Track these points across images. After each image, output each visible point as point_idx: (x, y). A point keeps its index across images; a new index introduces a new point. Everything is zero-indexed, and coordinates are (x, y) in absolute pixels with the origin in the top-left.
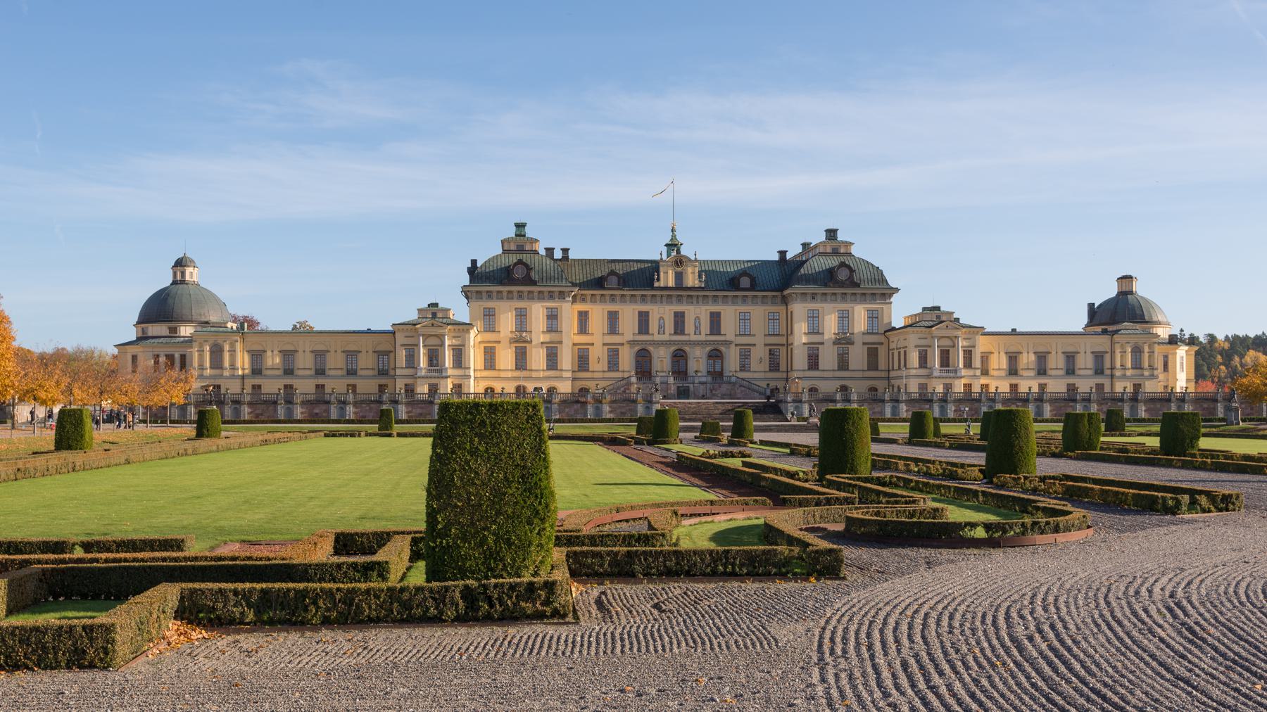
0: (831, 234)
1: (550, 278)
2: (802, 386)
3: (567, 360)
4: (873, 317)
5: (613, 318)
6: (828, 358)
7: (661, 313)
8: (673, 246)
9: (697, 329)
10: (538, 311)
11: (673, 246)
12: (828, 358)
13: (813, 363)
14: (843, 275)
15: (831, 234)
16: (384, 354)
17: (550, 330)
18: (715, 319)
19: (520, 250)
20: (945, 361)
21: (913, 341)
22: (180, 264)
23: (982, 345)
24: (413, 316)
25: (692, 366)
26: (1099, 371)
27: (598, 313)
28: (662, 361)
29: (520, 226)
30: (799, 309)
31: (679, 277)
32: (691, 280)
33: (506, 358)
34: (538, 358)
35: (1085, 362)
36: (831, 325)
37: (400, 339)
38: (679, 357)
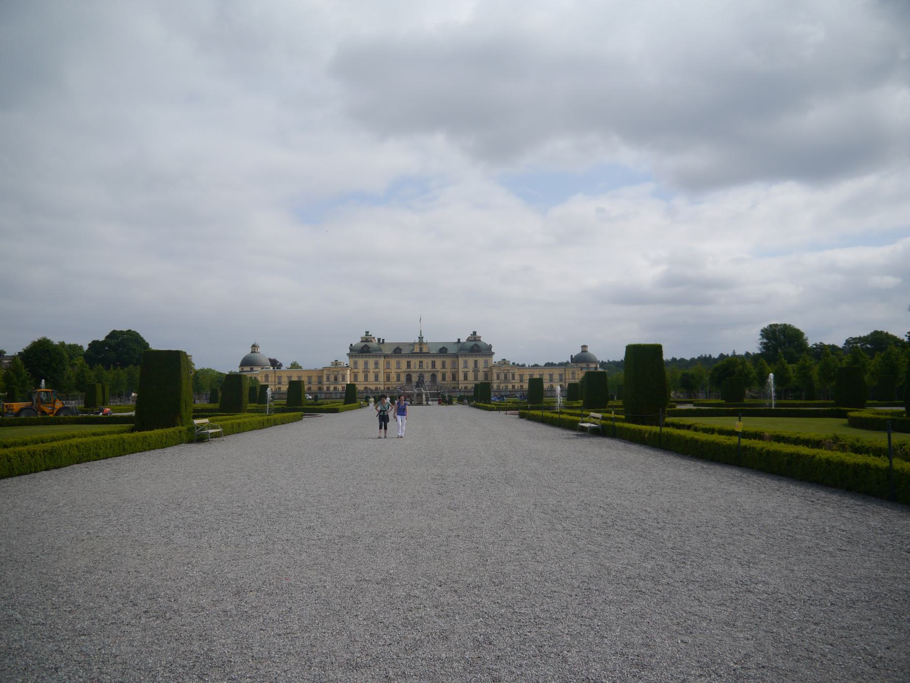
0: (475, 333)
1: (376, 350)
2: (461, 386)
3: (382, 377)
4: (486, 362)
5: (398, 363)
6: (471, 376)
7: (415, 362)
8: (421, 338)
9: (427, 367)
10: (371, 362)
11: (421, 338)
12: (471, 376)
13: (466, 378)
14: (476, 348)
15: (475, 333)
16: (320, 378)
17: (376, 368)
18: (434, 364)
19: (367, 341)
20: (506, 377)
21: (495, 371)
22: (254, 346)
23: (517, 373)
24: (329, 365)
25: (426, 379)
26: (561, 380)
27: (393, 362)
28: (415, 378)
29: (367, 332)
30: (461, 360)
31: (421, 349)
32: (425, 350)
33: (361, 377)
34: (371, 377)
35: (556, 377)
36: (471, 365)
37: (325, 372)
38: (421, 376)
